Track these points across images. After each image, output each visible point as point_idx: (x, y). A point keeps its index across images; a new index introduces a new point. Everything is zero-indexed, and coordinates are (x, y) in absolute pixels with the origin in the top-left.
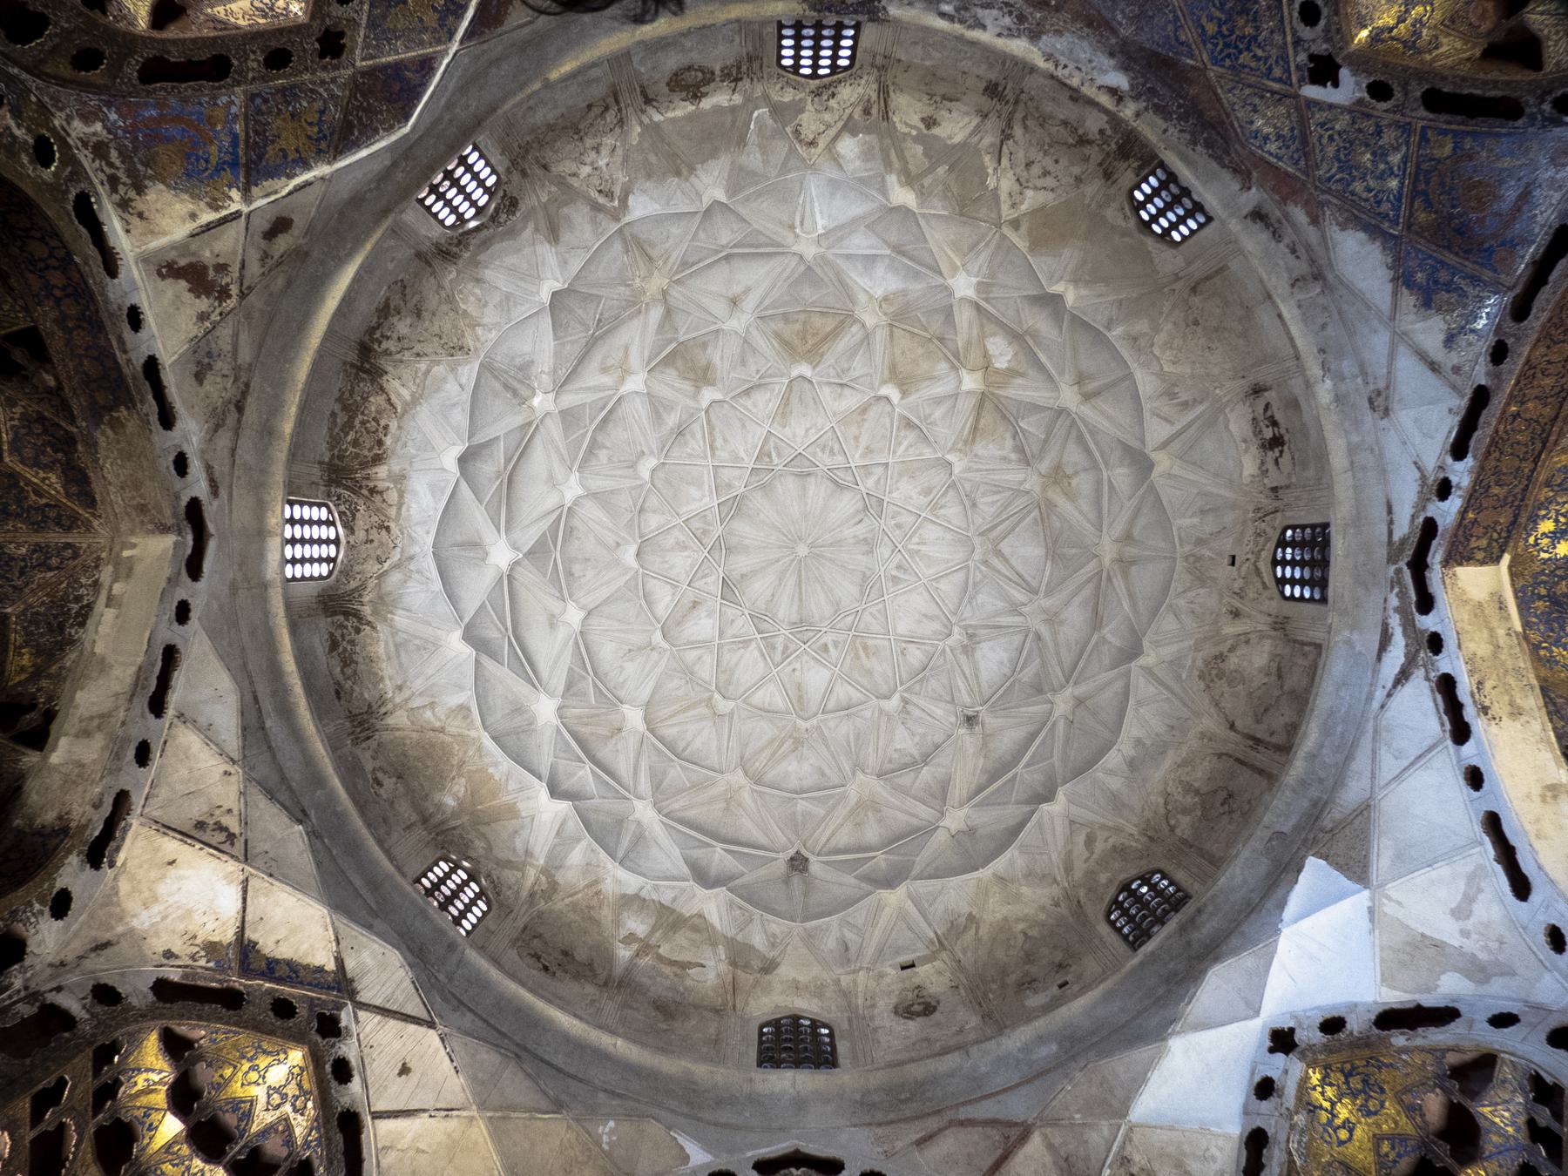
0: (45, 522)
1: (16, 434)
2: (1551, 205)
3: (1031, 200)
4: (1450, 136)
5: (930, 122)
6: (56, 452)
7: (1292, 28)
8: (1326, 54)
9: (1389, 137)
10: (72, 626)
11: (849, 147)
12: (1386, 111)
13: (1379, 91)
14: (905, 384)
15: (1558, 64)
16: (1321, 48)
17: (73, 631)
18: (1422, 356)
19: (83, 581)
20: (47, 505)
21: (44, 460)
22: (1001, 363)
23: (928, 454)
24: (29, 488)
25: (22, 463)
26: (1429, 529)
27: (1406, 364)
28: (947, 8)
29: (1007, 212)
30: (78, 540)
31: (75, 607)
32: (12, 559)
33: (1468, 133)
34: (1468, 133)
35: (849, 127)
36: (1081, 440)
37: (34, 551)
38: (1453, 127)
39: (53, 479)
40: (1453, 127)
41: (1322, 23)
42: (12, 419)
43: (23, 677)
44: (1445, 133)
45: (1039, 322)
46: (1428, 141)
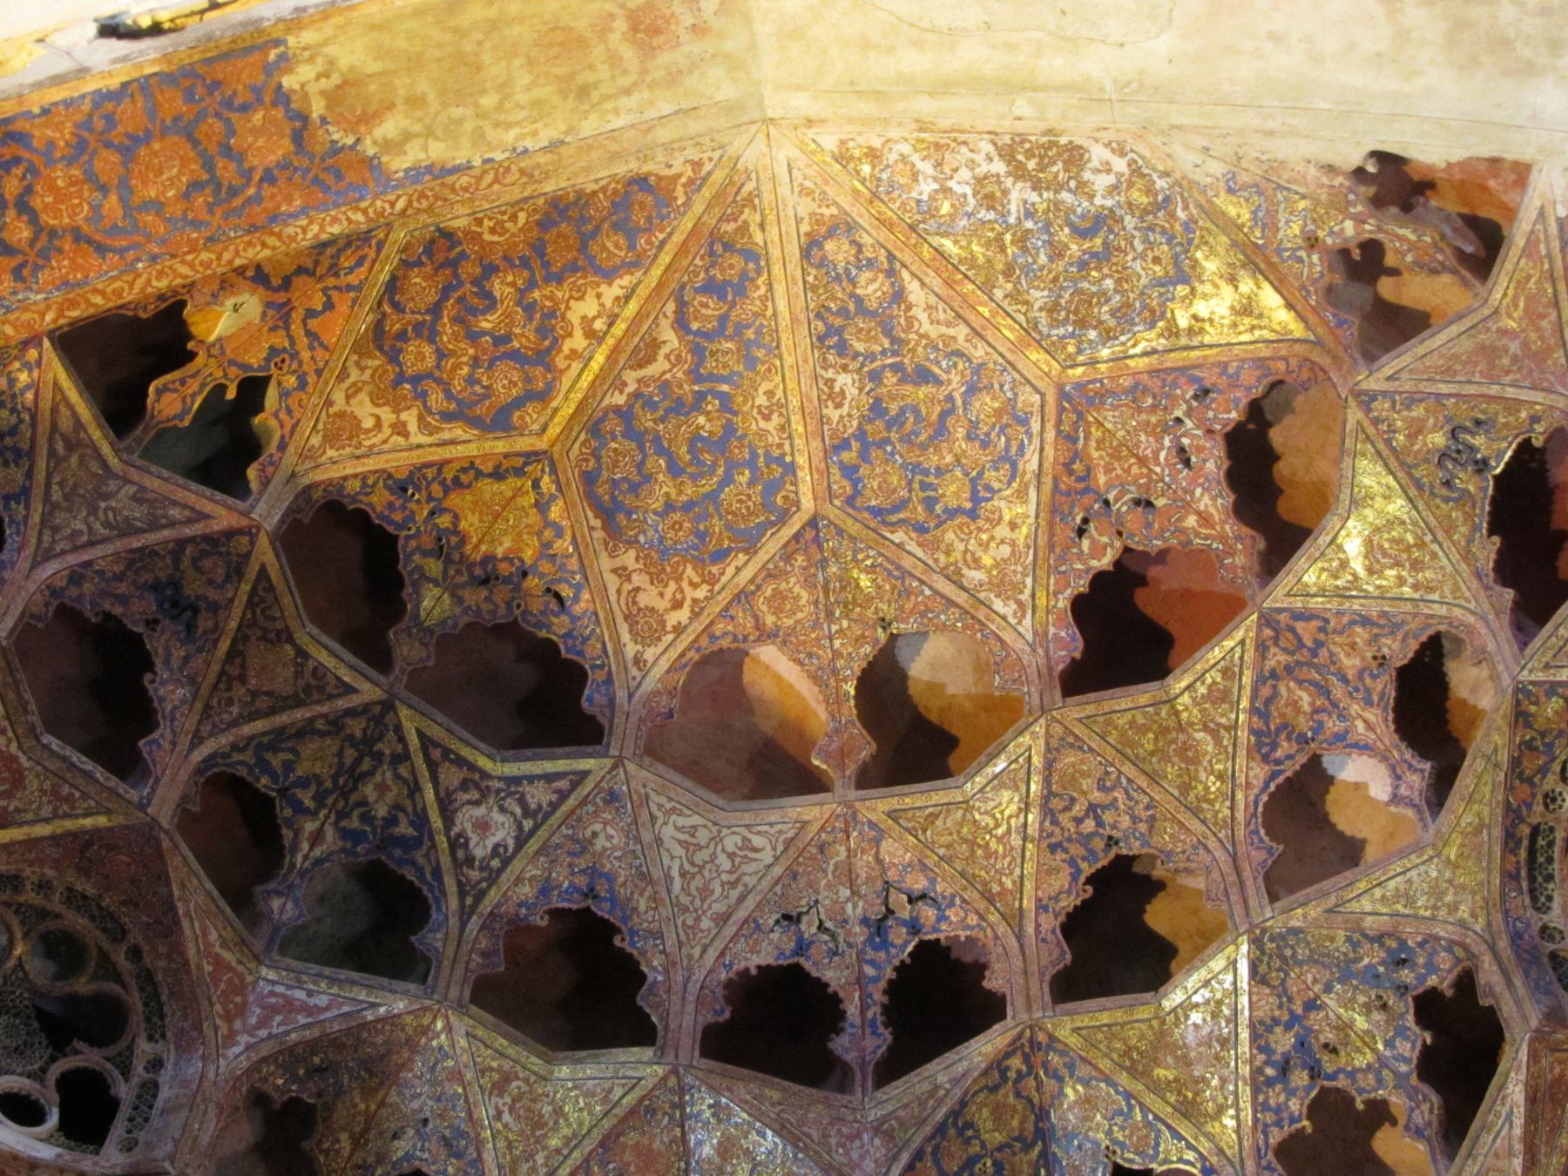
0: (740, 329)
1: (447, 417)
6: (491, 303)
10: (1083, 189)
17: (1102, 182)
19: (926, 188)
20: (681, 323)
21: (524, 336)
24: (631, 377)
25: (543, 396)
30: (789, 226)
31: (1019, 194)
32: (877, 408)
37: (842, 348)
39: (588, 307)
42: (400, 429)
43: (1270, 298)
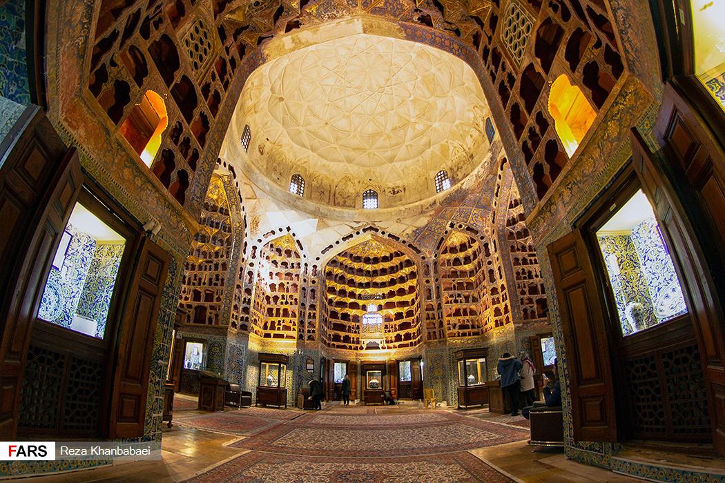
3: (451, 148)
5: (471, 136)
9: (440, 231)
11: (471, 115)
14: (414, 101)
16: (455, 227)
18: (405, 230)
22: (417, 126)
23: (395, 105)
26: (377, 230)
27: (405, 227)
28: (486, 164)
29: (449, 141)
35: (475, 118)
36: (398, 144)
45: (424, 140)
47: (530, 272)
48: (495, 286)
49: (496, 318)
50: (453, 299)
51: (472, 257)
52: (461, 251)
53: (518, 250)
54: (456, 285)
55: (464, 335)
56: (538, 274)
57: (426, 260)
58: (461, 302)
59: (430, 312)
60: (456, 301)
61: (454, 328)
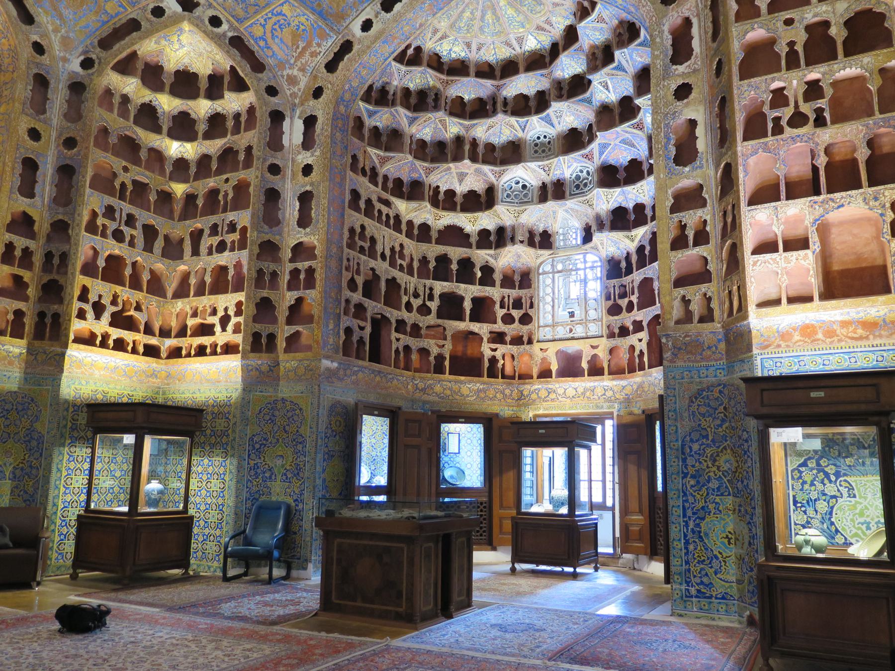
2: (48, 23)
4: (114, 15)
7: (218, 10)
8: (194, 11)
12: (148, 5)
13: (158, 12)
15: (108, 75)
16: (198, 11)
33: (108, 21)
34: (108, 21)
38: (117, 19)
40: (117, 19)
41: (207, 22)
44: (117, 15)
46: (120, 6)
47: (373, 240)
48: (275, 239)
49: (258, 327)
50: (112, 226)
51: (202, 128)
52: (176, 92)
53: (364, 173)
54: (130, 187)
55: (120, 345)
56: (388, 253)
57: (45, 59)
58: (132, 244)
59: (20, 242)
60: (118, 236)
61: (98, 317)
